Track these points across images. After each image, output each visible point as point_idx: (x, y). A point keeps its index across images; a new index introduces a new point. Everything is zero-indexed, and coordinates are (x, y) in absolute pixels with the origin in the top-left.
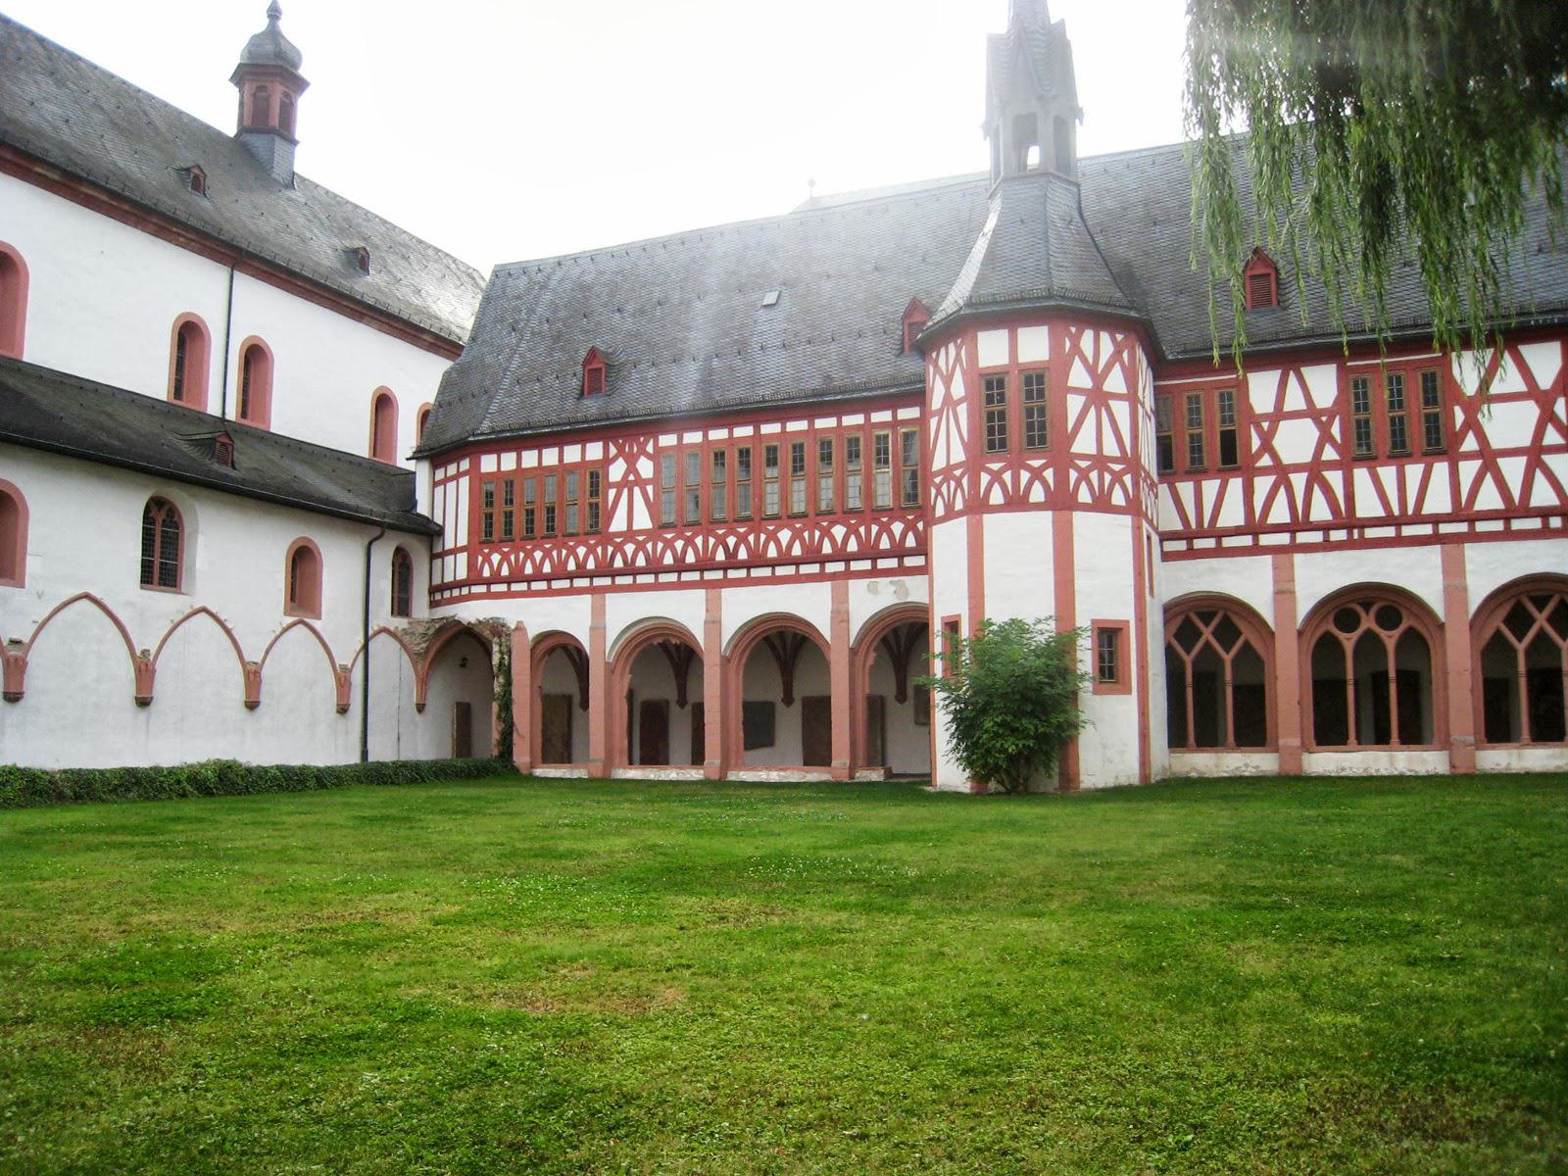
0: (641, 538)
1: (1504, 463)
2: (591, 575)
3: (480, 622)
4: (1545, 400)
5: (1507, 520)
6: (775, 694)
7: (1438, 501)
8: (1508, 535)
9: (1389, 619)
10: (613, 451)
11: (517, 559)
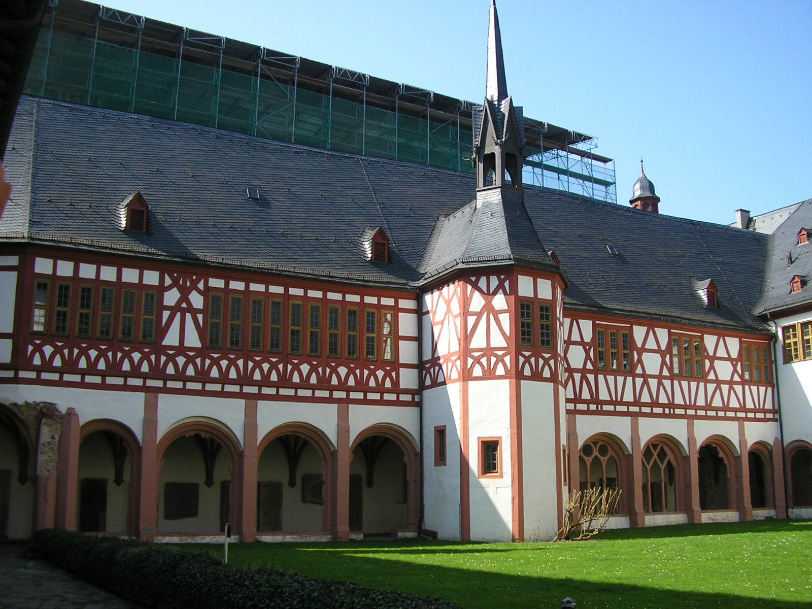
0: (191, 354)
2: (145, 377)
3: (27, 404)
6: (284, 478)
7: (629, 397)
8: (652, 415)
9: (603, 450)
10: (168, 281)
11: (71, 353)
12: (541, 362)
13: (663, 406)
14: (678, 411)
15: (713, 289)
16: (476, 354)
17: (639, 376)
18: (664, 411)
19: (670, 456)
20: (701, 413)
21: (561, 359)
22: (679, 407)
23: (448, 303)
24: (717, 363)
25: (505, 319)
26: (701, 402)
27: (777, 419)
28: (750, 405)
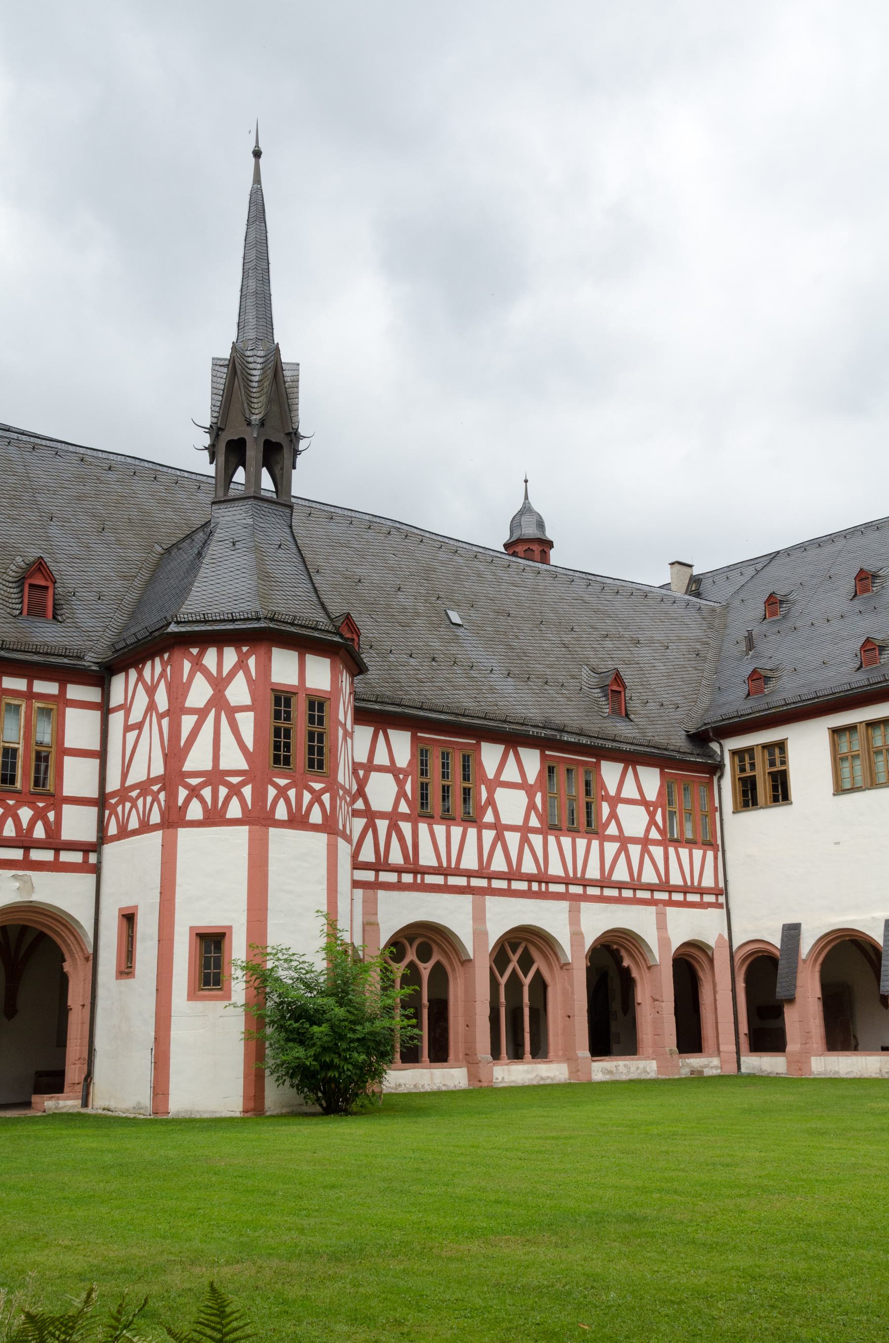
1: (507, 834)
4: (530, 791)
5: (509, 880)
7: (470, 862)
9: (424, 954)
12: (307, 797)
13: (530, 879)
14: (553, 888)
15: (619, 686)
16: (194, 782)
17: (489, 826)
18: (530, 887)
19: (539, 964)
20: (593, 891)
21: (344, 793)
22: (557, 880)
23: (151, 691)
24: (621, 809)
25: (246, 722)
26: (593, 873)
27: (723, 904)
28: (676, 879)
